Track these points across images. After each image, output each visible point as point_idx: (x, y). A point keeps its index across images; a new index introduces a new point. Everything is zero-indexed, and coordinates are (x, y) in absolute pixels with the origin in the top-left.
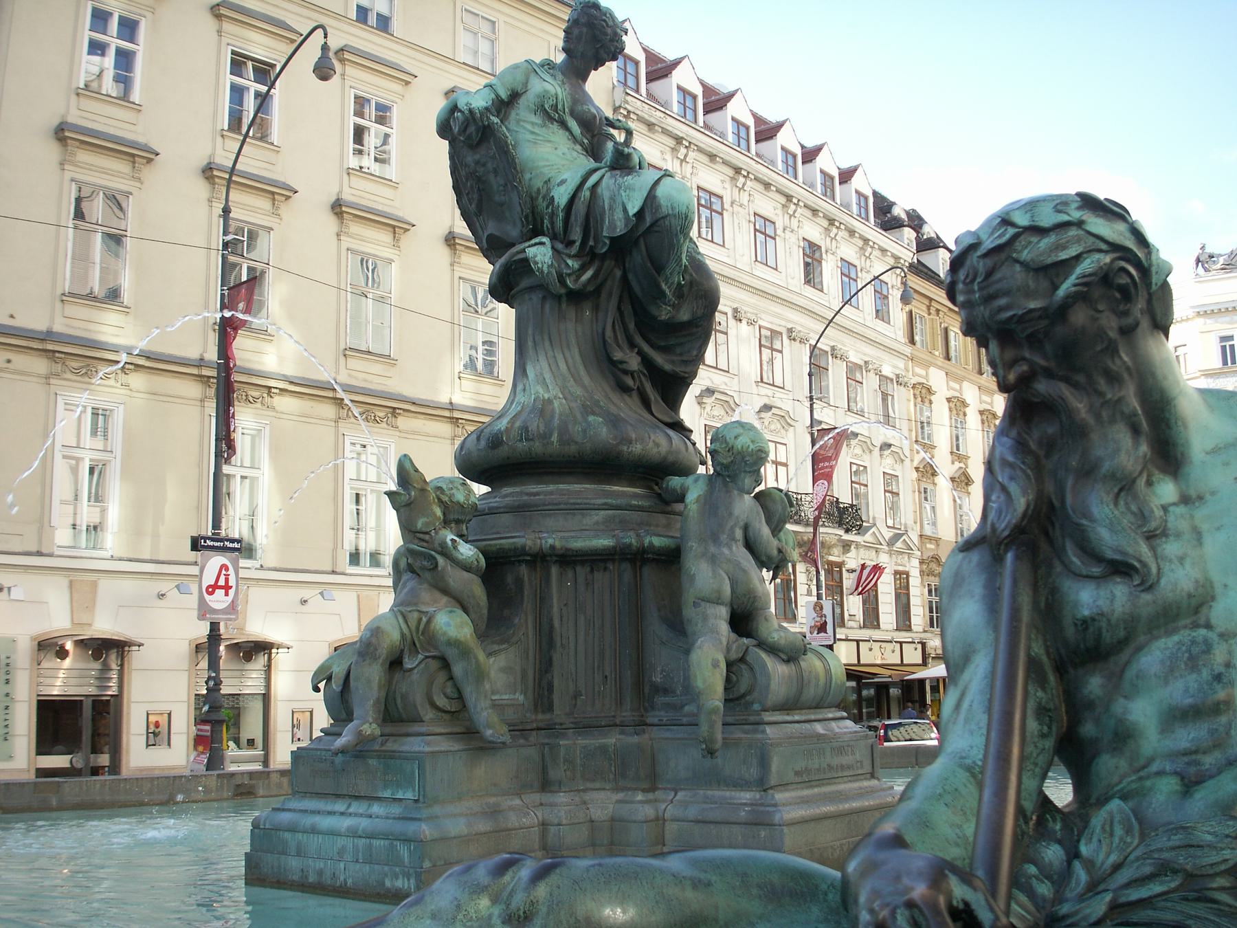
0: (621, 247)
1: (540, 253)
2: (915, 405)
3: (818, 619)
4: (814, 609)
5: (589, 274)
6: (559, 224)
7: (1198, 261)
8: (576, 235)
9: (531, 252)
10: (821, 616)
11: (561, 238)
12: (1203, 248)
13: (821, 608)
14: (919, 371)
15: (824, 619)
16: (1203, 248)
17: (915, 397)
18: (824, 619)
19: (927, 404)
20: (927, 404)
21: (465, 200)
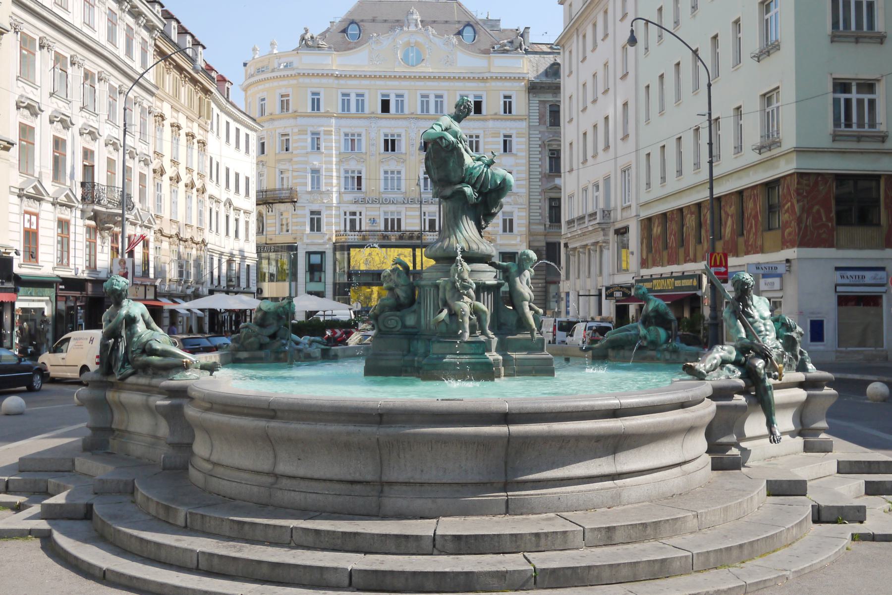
0: (491, 191)
1: (468, 190)
2: (155, 127)
3: (122, 270)
4: (120, 263)
5: (480, 199)
6: (473, 181)
7: (303, 39)
8: (478, 186)
9: (466, 189)
10: (124, 268)
11: (473, 186)
12: (307, 31)
13: (125, 263)
14: (159, 104)
15: (126, 270)
16: (307, 31)
17: (156, 122)
18: (126, 270)
19: (161, 126)
20: (161, 126)
21: (430, 163)
